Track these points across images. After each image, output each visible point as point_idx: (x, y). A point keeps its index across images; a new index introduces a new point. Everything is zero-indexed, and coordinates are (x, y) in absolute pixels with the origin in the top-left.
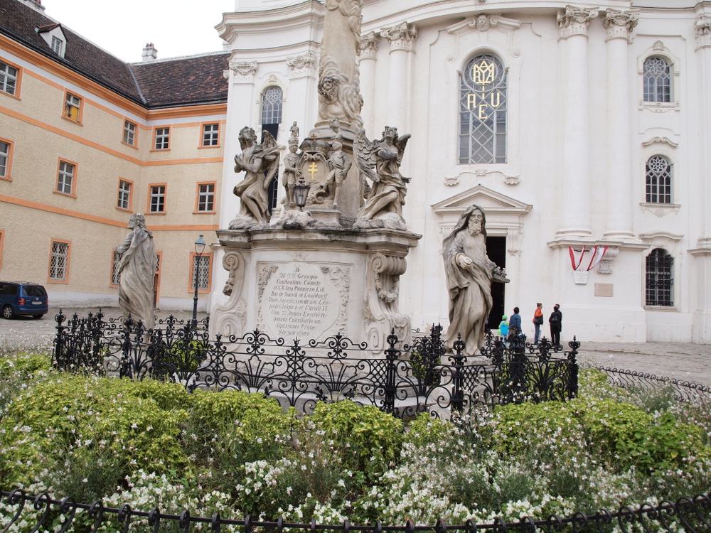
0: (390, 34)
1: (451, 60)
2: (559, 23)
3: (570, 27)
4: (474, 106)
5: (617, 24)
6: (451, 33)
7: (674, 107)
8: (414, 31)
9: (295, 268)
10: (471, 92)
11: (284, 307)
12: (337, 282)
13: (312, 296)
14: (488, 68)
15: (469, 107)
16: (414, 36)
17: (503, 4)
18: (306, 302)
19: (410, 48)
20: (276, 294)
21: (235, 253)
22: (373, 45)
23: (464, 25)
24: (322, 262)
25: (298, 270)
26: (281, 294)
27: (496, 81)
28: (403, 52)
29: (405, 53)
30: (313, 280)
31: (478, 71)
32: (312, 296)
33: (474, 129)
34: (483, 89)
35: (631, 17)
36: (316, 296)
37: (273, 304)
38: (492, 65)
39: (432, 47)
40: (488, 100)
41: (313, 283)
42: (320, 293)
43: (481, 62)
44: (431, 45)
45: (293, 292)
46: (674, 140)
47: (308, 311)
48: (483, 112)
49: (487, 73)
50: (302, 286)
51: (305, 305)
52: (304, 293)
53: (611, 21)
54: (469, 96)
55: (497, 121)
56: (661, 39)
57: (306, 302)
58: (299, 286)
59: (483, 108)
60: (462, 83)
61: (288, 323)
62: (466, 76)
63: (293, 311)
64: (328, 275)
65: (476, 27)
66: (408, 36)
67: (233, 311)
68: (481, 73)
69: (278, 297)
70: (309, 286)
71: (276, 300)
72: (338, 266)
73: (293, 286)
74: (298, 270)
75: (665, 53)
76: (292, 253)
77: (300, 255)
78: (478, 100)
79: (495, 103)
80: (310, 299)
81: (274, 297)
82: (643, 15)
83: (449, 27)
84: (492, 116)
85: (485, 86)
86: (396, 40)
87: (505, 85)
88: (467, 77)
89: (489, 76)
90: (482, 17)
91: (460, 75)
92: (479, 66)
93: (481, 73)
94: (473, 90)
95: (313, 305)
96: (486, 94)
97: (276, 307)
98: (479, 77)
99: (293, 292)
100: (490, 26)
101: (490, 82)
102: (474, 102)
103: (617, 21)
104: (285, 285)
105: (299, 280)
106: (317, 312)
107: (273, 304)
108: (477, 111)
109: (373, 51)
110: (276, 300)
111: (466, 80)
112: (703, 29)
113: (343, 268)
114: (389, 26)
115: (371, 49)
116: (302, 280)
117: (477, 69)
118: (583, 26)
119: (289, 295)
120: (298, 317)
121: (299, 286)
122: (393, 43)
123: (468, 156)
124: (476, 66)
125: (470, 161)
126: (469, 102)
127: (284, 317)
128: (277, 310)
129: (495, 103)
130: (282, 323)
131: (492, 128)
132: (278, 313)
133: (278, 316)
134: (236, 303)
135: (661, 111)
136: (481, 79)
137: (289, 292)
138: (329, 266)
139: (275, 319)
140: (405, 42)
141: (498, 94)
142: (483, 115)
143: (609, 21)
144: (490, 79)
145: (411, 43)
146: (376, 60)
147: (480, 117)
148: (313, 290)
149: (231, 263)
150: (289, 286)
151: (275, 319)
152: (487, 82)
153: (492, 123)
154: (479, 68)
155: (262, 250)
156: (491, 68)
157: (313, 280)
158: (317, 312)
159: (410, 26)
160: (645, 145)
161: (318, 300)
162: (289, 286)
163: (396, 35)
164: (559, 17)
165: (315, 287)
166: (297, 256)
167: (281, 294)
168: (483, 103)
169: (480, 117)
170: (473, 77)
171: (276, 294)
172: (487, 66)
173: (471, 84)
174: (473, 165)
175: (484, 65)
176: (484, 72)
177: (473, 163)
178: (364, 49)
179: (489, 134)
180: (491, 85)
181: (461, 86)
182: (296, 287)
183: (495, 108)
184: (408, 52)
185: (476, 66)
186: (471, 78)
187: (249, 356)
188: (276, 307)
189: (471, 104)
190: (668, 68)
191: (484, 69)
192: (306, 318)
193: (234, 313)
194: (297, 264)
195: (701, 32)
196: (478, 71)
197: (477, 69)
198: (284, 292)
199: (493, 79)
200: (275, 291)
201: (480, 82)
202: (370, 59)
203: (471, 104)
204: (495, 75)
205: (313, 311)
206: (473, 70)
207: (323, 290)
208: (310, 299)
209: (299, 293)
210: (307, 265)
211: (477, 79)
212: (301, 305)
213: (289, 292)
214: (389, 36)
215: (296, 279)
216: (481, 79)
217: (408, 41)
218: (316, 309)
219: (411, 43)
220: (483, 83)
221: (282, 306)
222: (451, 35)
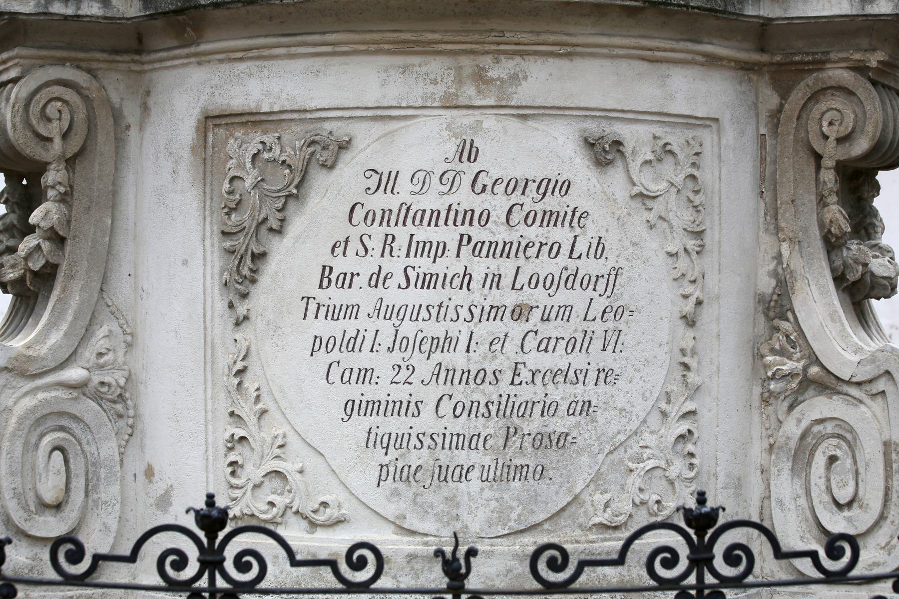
9: (451, 148)
11: (398, 343)
12: (658, 206)
13: (549, 283)
18: (520, 312)
20: (347, 280)
21: (68, 73)
24: (586, 112)
26: (378, 279)
30: (552, 203)
32: (549, 283)
36: (571, 280)
37: (325, 328)
41: (551, 218)
42: (590, 267)
45: (451, 265)
47: (535, 360)
50: (498, 233)
51: (517, 330)
52: (507, 267)
57: (520, 312)
58: (478, 233)
61: (427, 422)
63: (458, 359)
64: (616, 176)
67: (74, 374)
70: (534, 233)
71: (352, 311)
72: (658, 130)
73: (449, 235)
76: (436, 66)
77: (480, 78)
80: (539, 296)
81: (336, 296)
95: (551, 329)
97: (352, 344)
99: (451, 265)
104: (402, 234)
105: (478, 203)
106: (578, 360)
107: (325, 328)
110: (352, 311)
113: (676, 139)
116: (498, 204)
119: (427, 281)
120: (489, 392)
121: (478, 233)
127: (400, 393)
128: (363, 359)
130: (395, 425)
132: (365, 375)
133: (372, 392)
134: (84, 339)
137: (424, 264)
138: (623, 131)
139: (350, 408)
148: (554, 250)
149: (54, 130)
150: (424, 233)
151: (350, 408)
155: (231, 57)
157: (552, 203)
158: (578, 360)
161: (577, 298)
162: (424, 233)
165: (561, 235)
166: (459, 81)
167: (378, 279)
171: (347, 280)
182: (464, 240)
188: (352, 344)
192: (526, 393)
193: (80, 387)
194: (464, 119)
198: (395, 266)
200: (341, 265)
205: (557, 360)
207: (599, 248)
208: (539, 296)
209: (480, 267)
210: (514, 125)
212: (497, 328)
213: (424, 264)
215: (464, 198)
218: (572, 345)
221: (386, 339)
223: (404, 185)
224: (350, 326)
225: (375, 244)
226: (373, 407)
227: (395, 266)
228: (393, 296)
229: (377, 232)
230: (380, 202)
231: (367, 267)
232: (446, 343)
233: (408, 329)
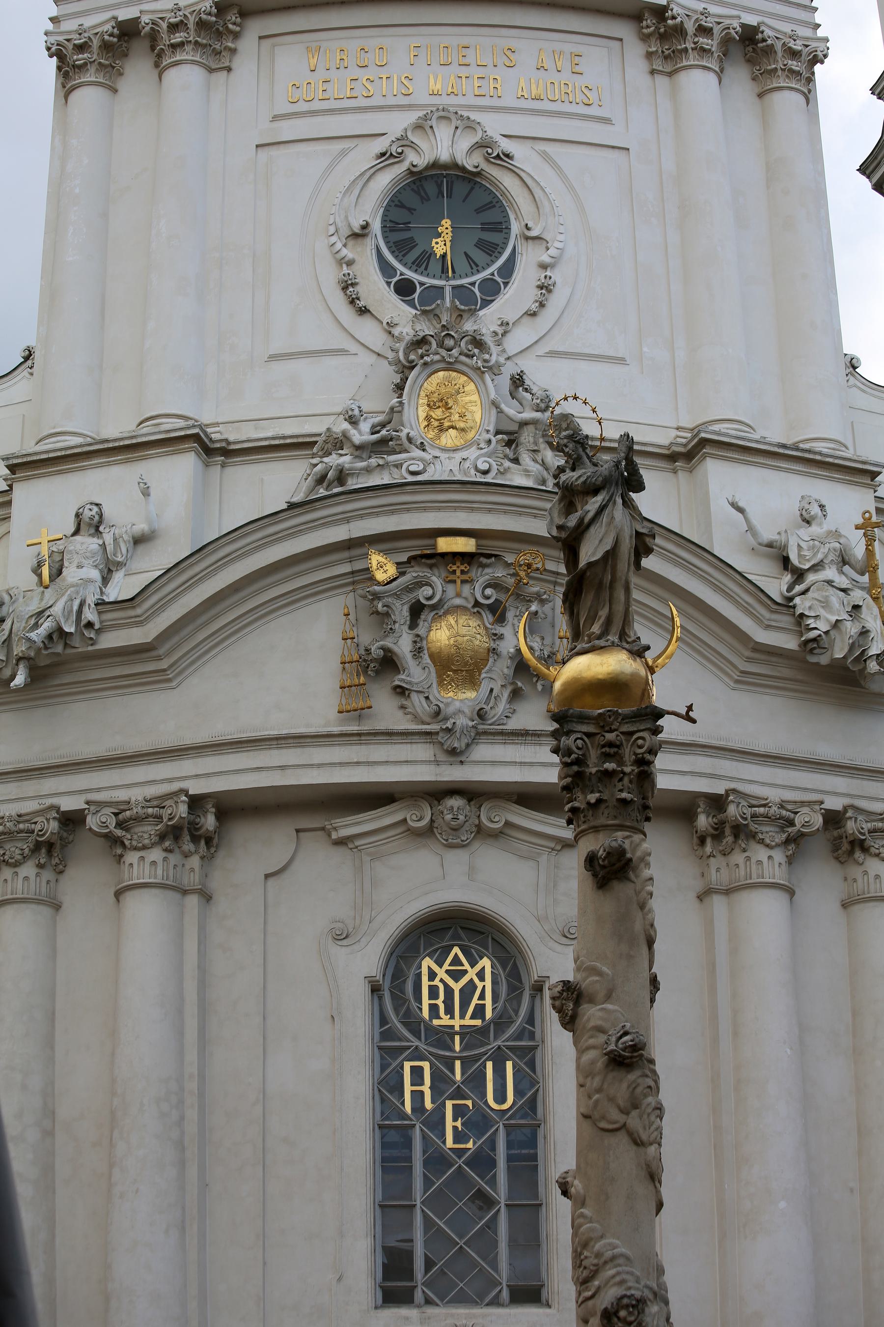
0: (119, 825)
1: (341, 937)
2: (702, 841)
3: (738, 858)
4: (428, 1105)
6: (341, 842)
8: (210, 821)
10: (418, 1055)
14: (472, 974)
15: (408, 1108)
16: (209, 841)
17: (526, 769)
19: (192, 879)
22: (49, 853)
23: (388, 821)
27: (501, 1022)
28: (170, 894)
29: (176, 896)
31: (437, 982)
33: (427, 1183)
34: (457, 1048)
38: (486, 963)
39: (271, 882)
40: (477, 1081)
43: (448, 949)
44: (267, 876)
48: (459, 1124)
49: (468, 991)
53: (859, 845)
54: (407, 1065)
55: (510, 1159)
59: (459, 1112)
60: (384, 1020)
62: (394, 996)
65: (429, 831)
66: (187, 837)
68: (449, 991)
78: (440, 1082)
79: (501, 1097)
83: (339, 822)
84: (492, 1143)
85: (463, 1035)
86: (144, 848)
87: (532, 1036)
88: (399, 1000)
89: (475, 1001)
90: (456, 802)
91: (375, 989)
92: (441, 966)
93: (449, 991)
94: (422, 1046)
96: (466, 1063)
98: (440, 1002)
100: (480, 831)
101: (478, 1022)
102: (426, 1089)
108: (436, 1122)
109: (48, 874)
111: (396, 1010)
114: (121, 795)
115: (40, 866)
117: (432, 975)
118: (779, 856)
122: (132, 857)
123: (410, 1276)
124: (427, 963)
125: (418, 1296)
126: (408, 1088)
129: (501, 1097)
131: (493, 1182)
136: (449, 1011)
140: (174, 858)
141: (509, 1065)
142: (459, 1137)
143: (852, 843)
144: (479, 1012)
145: (195, 861)
146: (57, 907)
147: (450, 1142)
152: (468, 1021)
153: (493, 1163)
154: (441, 973)
156: (481, 975)
159: (196, 802)
163: (147, 831)
164: (703, 821)
168: (458, 1094)
169: (450, 1142)
170: (419, 999)
172: (467, 966)
173: (414, 1024)
174: (431, 1311)
175: (456, 961)
176: (457, 987)
177: (428, 1302)
178: (17, 864)
179: (485, 1201)
180: (483, 1031)
181: (377, 1031)
183: (504, 1112)
184: (185, 892)
185: (427, 963)
186: (414, 1004)
189: (418, 1096)
191: (456, 975)
196: (437, 982)
197: (432, 975)
199: (489, 1014)
201: (444, 1020)
202: (38, 902)
203: (418, 1096)
204: (495, 999)
206: (419, 976)
211: (434, 1009)
214: (119, 833)
216: (449, 1011)
217: (186, 856)
219: (195, 861)
220: (457, 1023)
222: (342, 850)
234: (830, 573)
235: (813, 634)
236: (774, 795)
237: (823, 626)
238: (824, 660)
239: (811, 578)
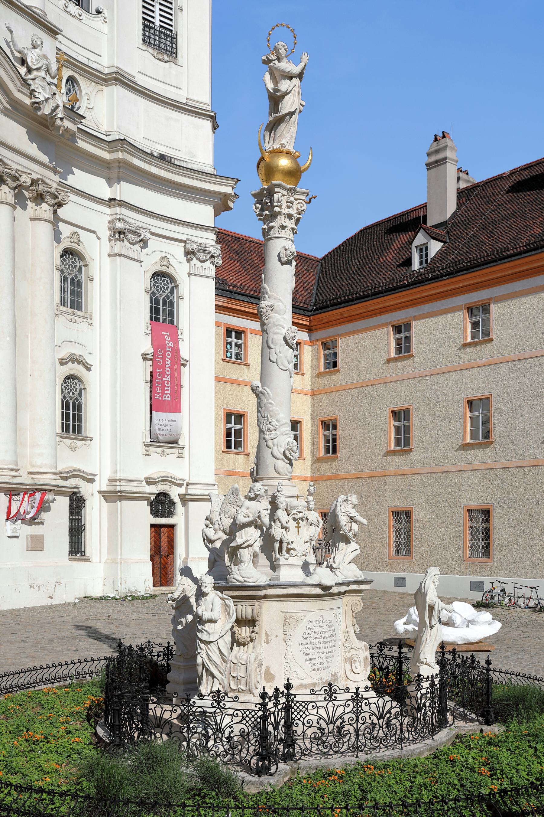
5: (46, 202)
7: (87, 318)
20: (306, 639)
25: (322, 616)
26: (310, 638)
35: (60, 197)
37: (303, 647)
45: (319, 635)
46: (89, 360)
56: (80, 231)
63: (320, 651)
69: (308, 641)
71: (306, 644)
74: (322, 616)
75: (80, 248)
81: (304, 641)
82: (73, 197)
97: (307, 649)
103: (48, 198)
107: (303, 647)
110: (306, 644)
112: (120, 233)
119: (317, 638)
121: (323, 630)
132: (309, 654)
135: (76, 322)
137: (316, 636)
160: (63, 362)
162: (316, 631)
171: (306, 639)
187: (377, 699)
190: (80, 268)
195: (117, 235)
200: (305, 636)
209: (323, 635)
215: (321, 625)
223: (314, 623)
224: (306, 646)
225: (310, 633)
226: (310, 659)
227: (312, 636)
228: (312, 641)
229: (310, 631)
230: (310, 626)
231: (308, 636)
232: (319, 648)
233: (314, 646)
234: (42, 74)
235: (38, 100)
236: (15, 166)
237: (42, 99)
238: (39, 113)
239: (35, 73)
